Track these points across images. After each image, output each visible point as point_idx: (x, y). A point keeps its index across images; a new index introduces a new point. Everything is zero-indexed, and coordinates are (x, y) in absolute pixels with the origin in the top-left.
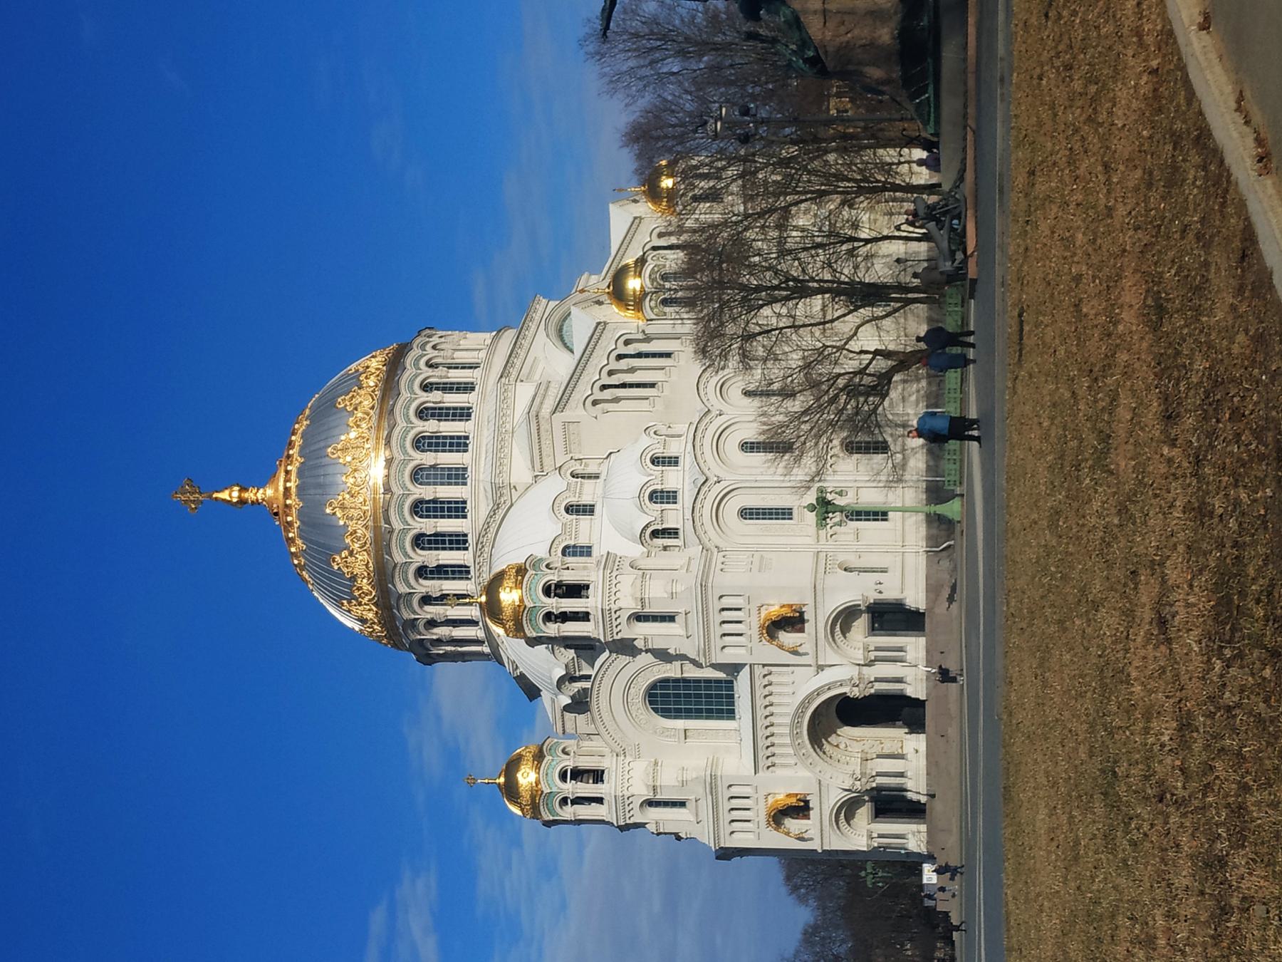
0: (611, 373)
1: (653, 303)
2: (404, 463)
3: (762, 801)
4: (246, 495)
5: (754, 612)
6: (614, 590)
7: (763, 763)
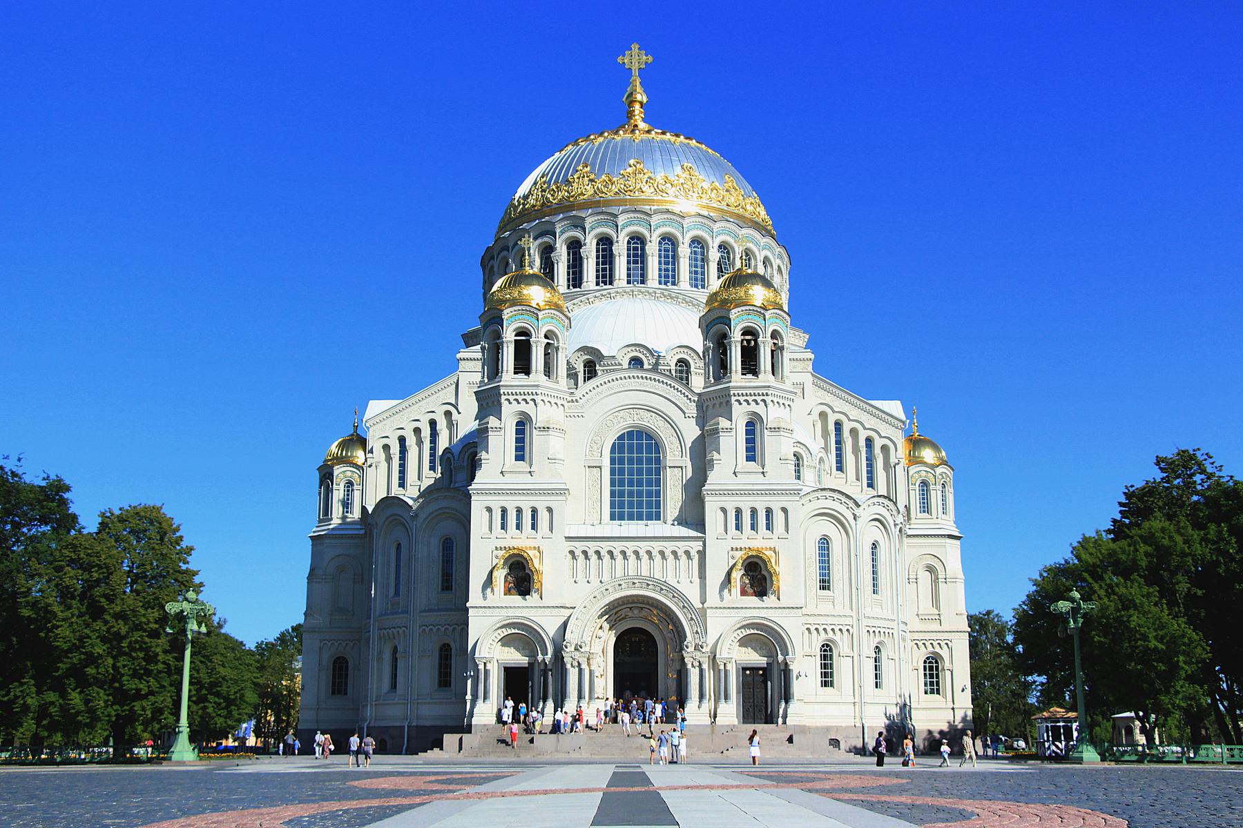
0: (854, 432)
1: (924, 474)
2: (736, 236)
3: (532, 543)
4: (637, 107)
5: (771, 544)
6: (781, 401)
7: (579, 547)
